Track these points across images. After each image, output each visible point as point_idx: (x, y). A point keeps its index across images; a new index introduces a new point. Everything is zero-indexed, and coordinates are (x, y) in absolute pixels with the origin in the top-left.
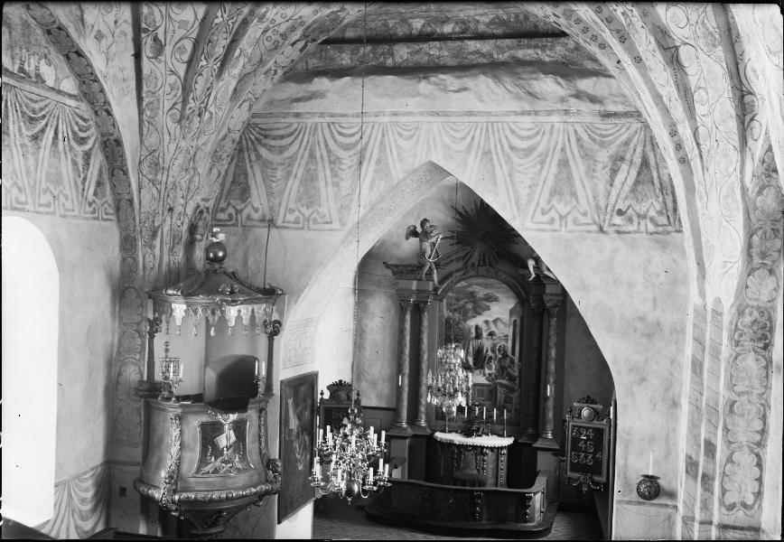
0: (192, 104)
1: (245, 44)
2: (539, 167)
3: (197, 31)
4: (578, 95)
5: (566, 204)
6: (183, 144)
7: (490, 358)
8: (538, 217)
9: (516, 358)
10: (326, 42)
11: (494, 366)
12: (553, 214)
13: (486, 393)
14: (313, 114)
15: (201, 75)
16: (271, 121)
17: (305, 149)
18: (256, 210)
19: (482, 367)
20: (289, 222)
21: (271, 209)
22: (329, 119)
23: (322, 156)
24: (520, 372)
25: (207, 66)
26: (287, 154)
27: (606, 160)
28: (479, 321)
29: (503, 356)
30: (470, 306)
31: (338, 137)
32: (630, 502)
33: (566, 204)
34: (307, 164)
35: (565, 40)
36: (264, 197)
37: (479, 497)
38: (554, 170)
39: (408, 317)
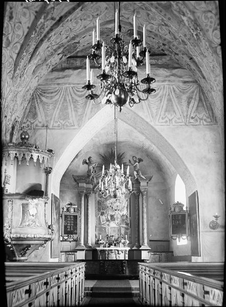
0: (18, 71)
1: (41, 49)
2: (160, 101)
3: (22, 41)
4: (173, 75)
5: (171, 115)
6: (13, 88)
8: (161, 120)
10: (69, 57)
12: (166, 119)
14: (66, 84)
15: (23, 59)
16: (47, 86)
17: (62, 97)
18: (40, 123)
20: (55, 127)
21: (47, 121)
22: (72, 86)
23: (69, 100)
24: (130, 221)
25: (26, 56)
26: (54, 99)
27: (186, 98)
31: (77, 92)
32: (206, 232)
33: (171, 115)
34: (63, 103)
35: (166, 57)
36: (43, 117)
37: (125, 263)
38: (166, 102)
39: (83, 199)
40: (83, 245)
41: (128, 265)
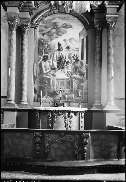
7: (68, 62)
9: (84, 61)
11: (70, 67)
13: (66, 84)
24: (87, 70)
28: (60, 40)
29: (76, 61)
30: (54, 31)
41: (93, 140)
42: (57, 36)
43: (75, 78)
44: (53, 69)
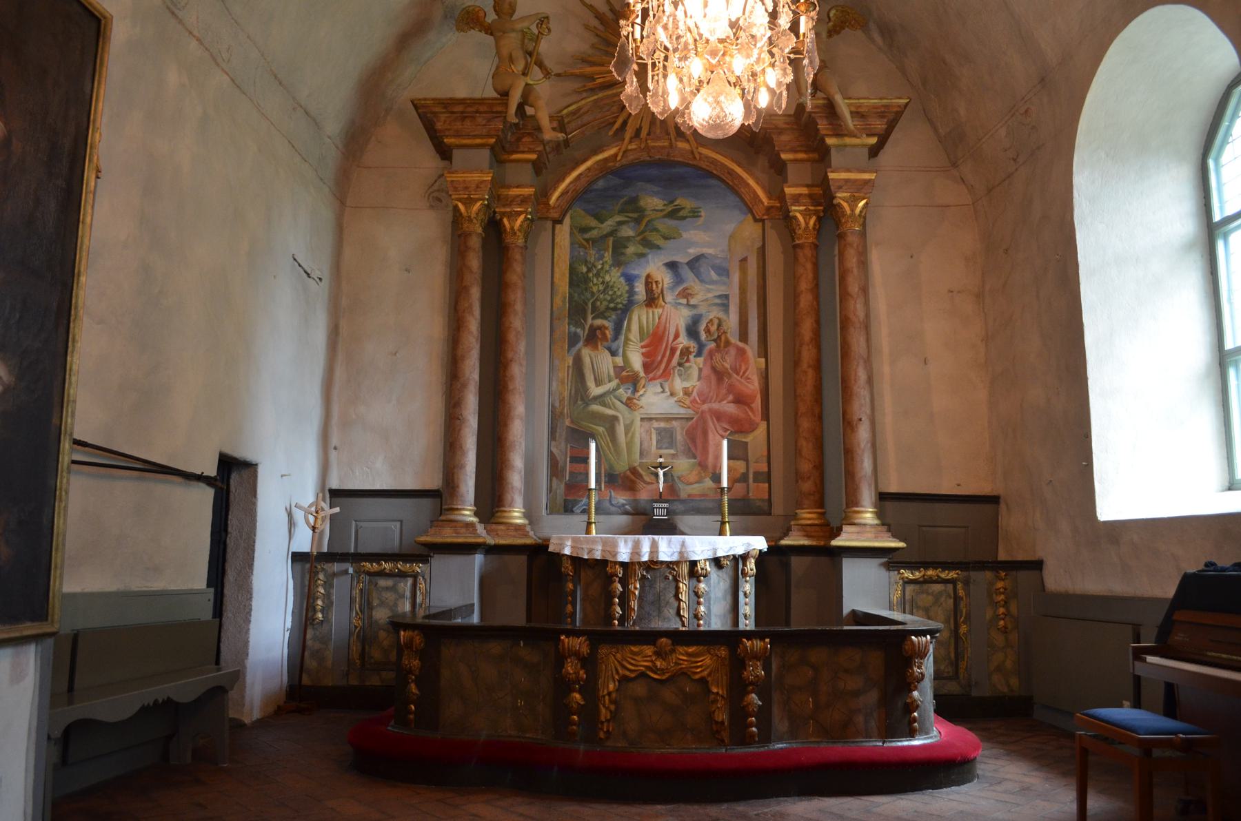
9: (751, 349)
11: (695, 373)
13: (680, 437)
19: (666, 375)
29: (718, 346)
40: (468, 514)
42: (641, 249)
43: (719, 416)
44: (632, 381)
